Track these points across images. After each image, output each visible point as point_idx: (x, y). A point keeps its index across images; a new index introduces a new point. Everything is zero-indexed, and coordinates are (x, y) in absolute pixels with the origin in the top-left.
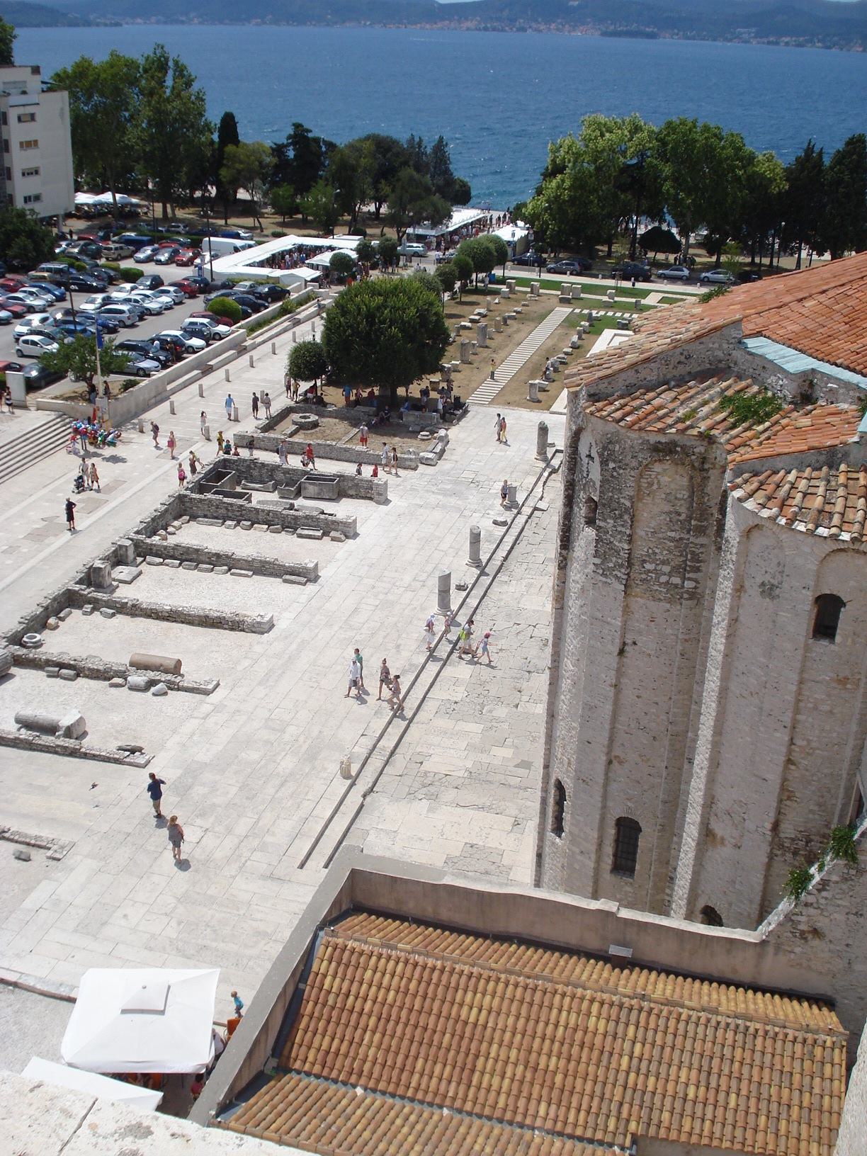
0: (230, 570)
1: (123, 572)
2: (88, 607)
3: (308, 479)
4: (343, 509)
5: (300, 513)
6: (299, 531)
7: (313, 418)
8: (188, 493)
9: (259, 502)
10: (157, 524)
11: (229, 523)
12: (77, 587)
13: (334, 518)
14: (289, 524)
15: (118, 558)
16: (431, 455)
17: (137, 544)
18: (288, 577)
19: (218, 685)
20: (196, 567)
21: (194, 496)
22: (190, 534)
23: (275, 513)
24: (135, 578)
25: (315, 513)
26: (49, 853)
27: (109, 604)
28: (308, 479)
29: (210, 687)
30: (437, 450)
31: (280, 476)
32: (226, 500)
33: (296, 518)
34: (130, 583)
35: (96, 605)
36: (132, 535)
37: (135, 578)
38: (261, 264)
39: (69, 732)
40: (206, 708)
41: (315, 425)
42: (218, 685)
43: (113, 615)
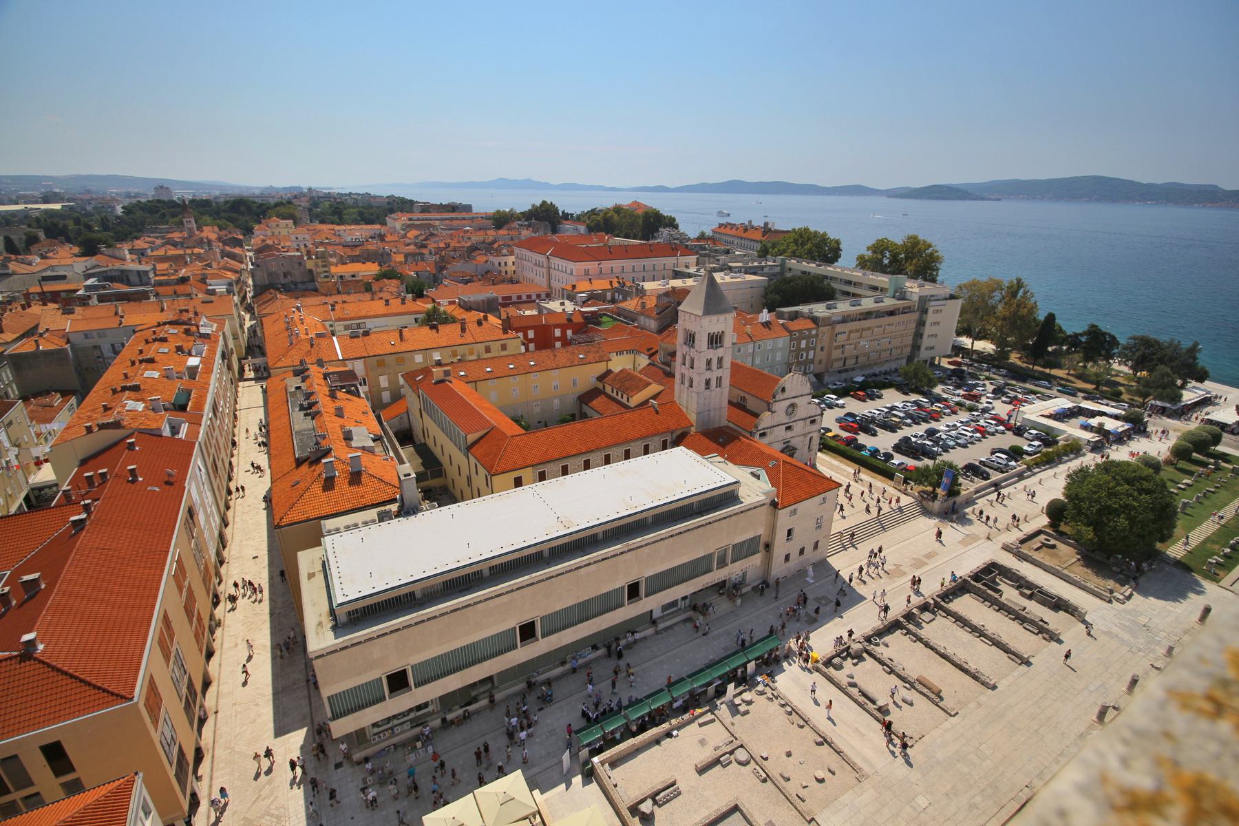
0: (980, 636)
1: (927, 616)
2: (905, 631)
3: (1038, 591)
4: (1055, 620)
5: (1028, 616)
6: (1025, 625)
7: (1053, 542)
8: (969, 579)
9: (1006, 599)
10: (949, 594)
11: (986, 603)
12: (902, 620)
13: (1045, 626)
14: (1019, 617)
15: (924, 608)
16: (1121, 597)
17: (936, 602)
18: (1011, 656)
19: (957, 713)
20: (962, 627)
21: (972, 582)
22: (965, 605)
23: (1014, 610)
24: (931, 621)
25: (1037, 620)
26: (857, 776)
27: (915, 635)
28: (1038, 591)
29: (953, 713)
30: (1127, 594)
31: (1023, 582)
32: (989, 592)
33: (1025, 617)
34: (928, 623)
35: (909, 632)
36: (935, 597)
37: (931, 621)
38: (1050, 417)
39: (880, 709)
40: (947, 725)
41: (1053, 547)
42: (957, 713)
43: (915, 641)
